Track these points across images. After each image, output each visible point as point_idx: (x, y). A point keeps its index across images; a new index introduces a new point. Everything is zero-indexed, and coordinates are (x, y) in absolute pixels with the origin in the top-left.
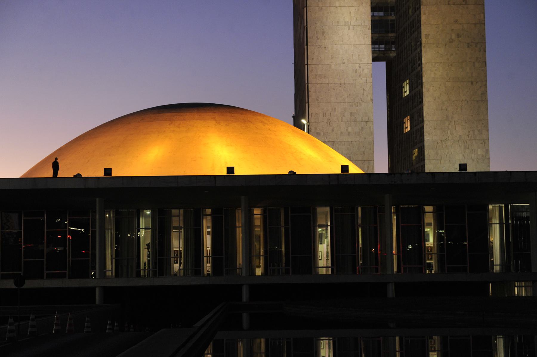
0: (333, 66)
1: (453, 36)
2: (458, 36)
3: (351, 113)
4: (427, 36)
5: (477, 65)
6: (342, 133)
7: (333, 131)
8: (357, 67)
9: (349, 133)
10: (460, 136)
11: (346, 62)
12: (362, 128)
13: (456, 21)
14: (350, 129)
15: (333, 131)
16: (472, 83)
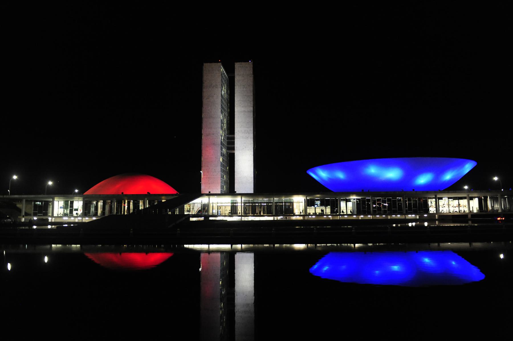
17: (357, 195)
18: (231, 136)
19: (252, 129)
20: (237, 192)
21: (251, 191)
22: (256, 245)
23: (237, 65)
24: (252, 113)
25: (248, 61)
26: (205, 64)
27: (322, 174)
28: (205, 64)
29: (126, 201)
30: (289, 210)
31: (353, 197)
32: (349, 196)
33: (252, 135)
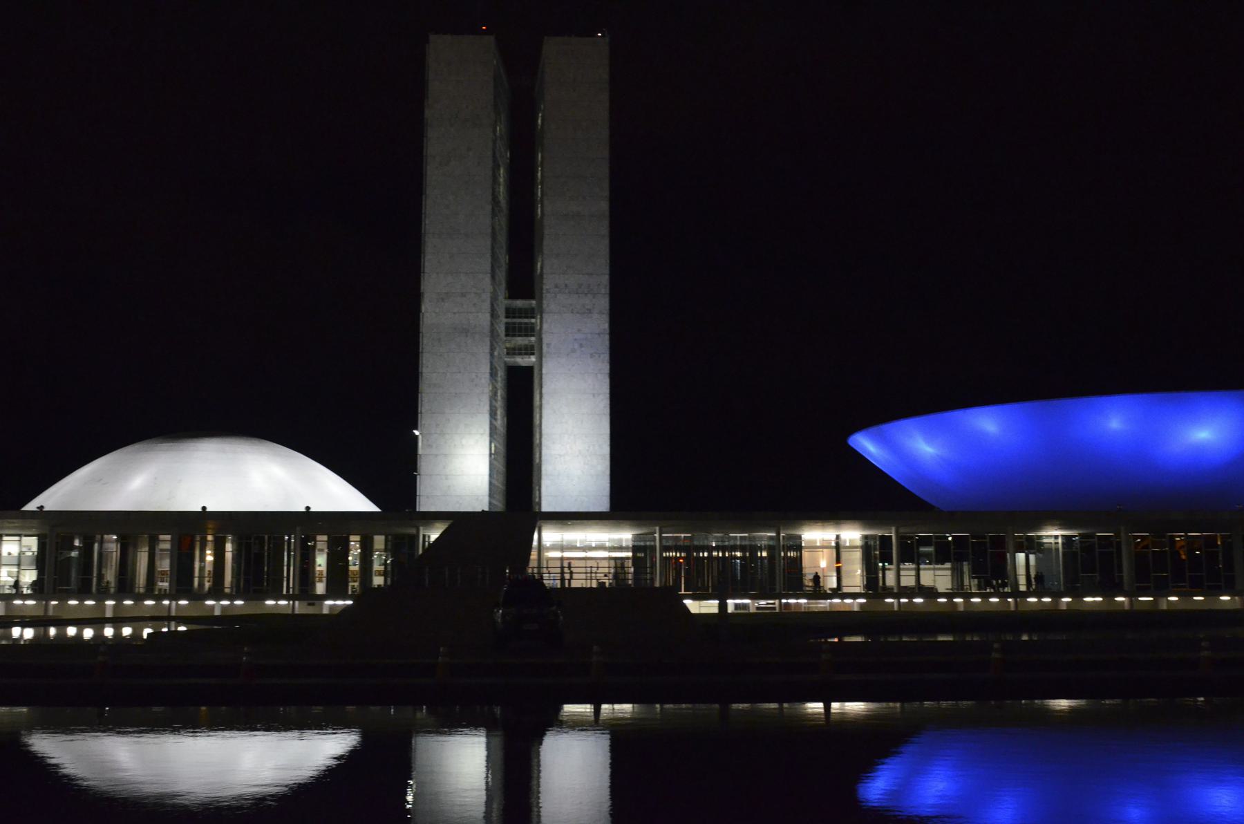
1: (576, 346)
2: (581, 346)
4: (548, 345)
8: (474, 376)
17: (1064, 526)
18: (519, 303)
19: (605, 279)
20: (546, 507)
21: (603, 505)
22: (703, 706)
24: (606, 223)
25: (595, 35)
26: (433, 37)
27: (914, 448)
28: (432, 37)
29: (210, 538)
30: (789, 574)
31: (1053, 535)
32: (1038, 525)
33: (604, 302)
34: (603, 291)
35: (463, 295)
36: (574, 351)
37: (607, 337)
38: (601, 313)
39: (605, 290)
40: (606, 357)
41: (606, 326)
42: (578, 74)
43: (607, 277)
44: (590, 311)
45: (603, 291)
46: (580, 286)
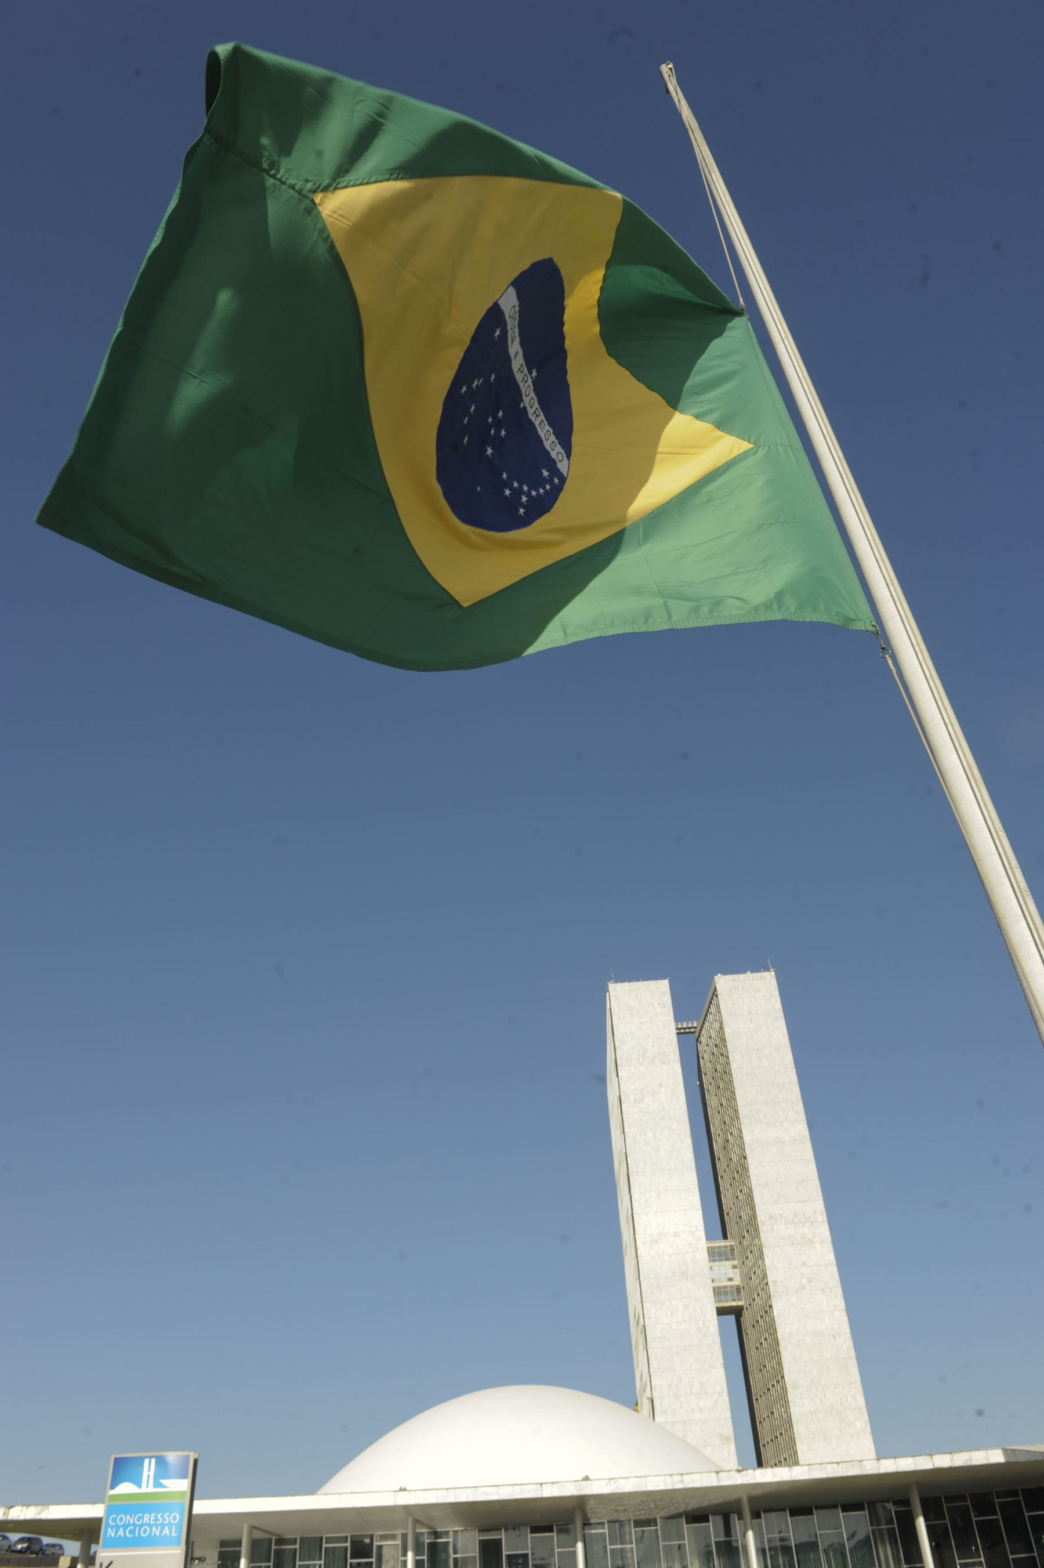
0: (674, 1326)
1: (804, 1281)
2: (809, 1281)
3: (701, 1384)
4: (775, 1282)
5: (836, 1314)
6: (692, 1409)
7: (681, 1407)
9: (701, 1410)
10: (832, 1405)
11: (687, 1319)
12: (716, 1401)
13: (804, 1264)
14: (701, 1403)
15: (681, 1407)
16: (834, 1337)
19: (820, 1205)
23: (723, 982)
28: (612, 987)
33: (824, 1231)
34: (820, 1218)
35: (676, 1235)
36: (803, 1287)
37: (835, 1268)
38: (822, 1242)
39: (822, 1217)
40: (839, 1291)
41: (831, 1256)
42: (751, 1007)
43: (822, 1202)
44: (811, 1241)
45: (820, 1218)
46: (795, 1215)
